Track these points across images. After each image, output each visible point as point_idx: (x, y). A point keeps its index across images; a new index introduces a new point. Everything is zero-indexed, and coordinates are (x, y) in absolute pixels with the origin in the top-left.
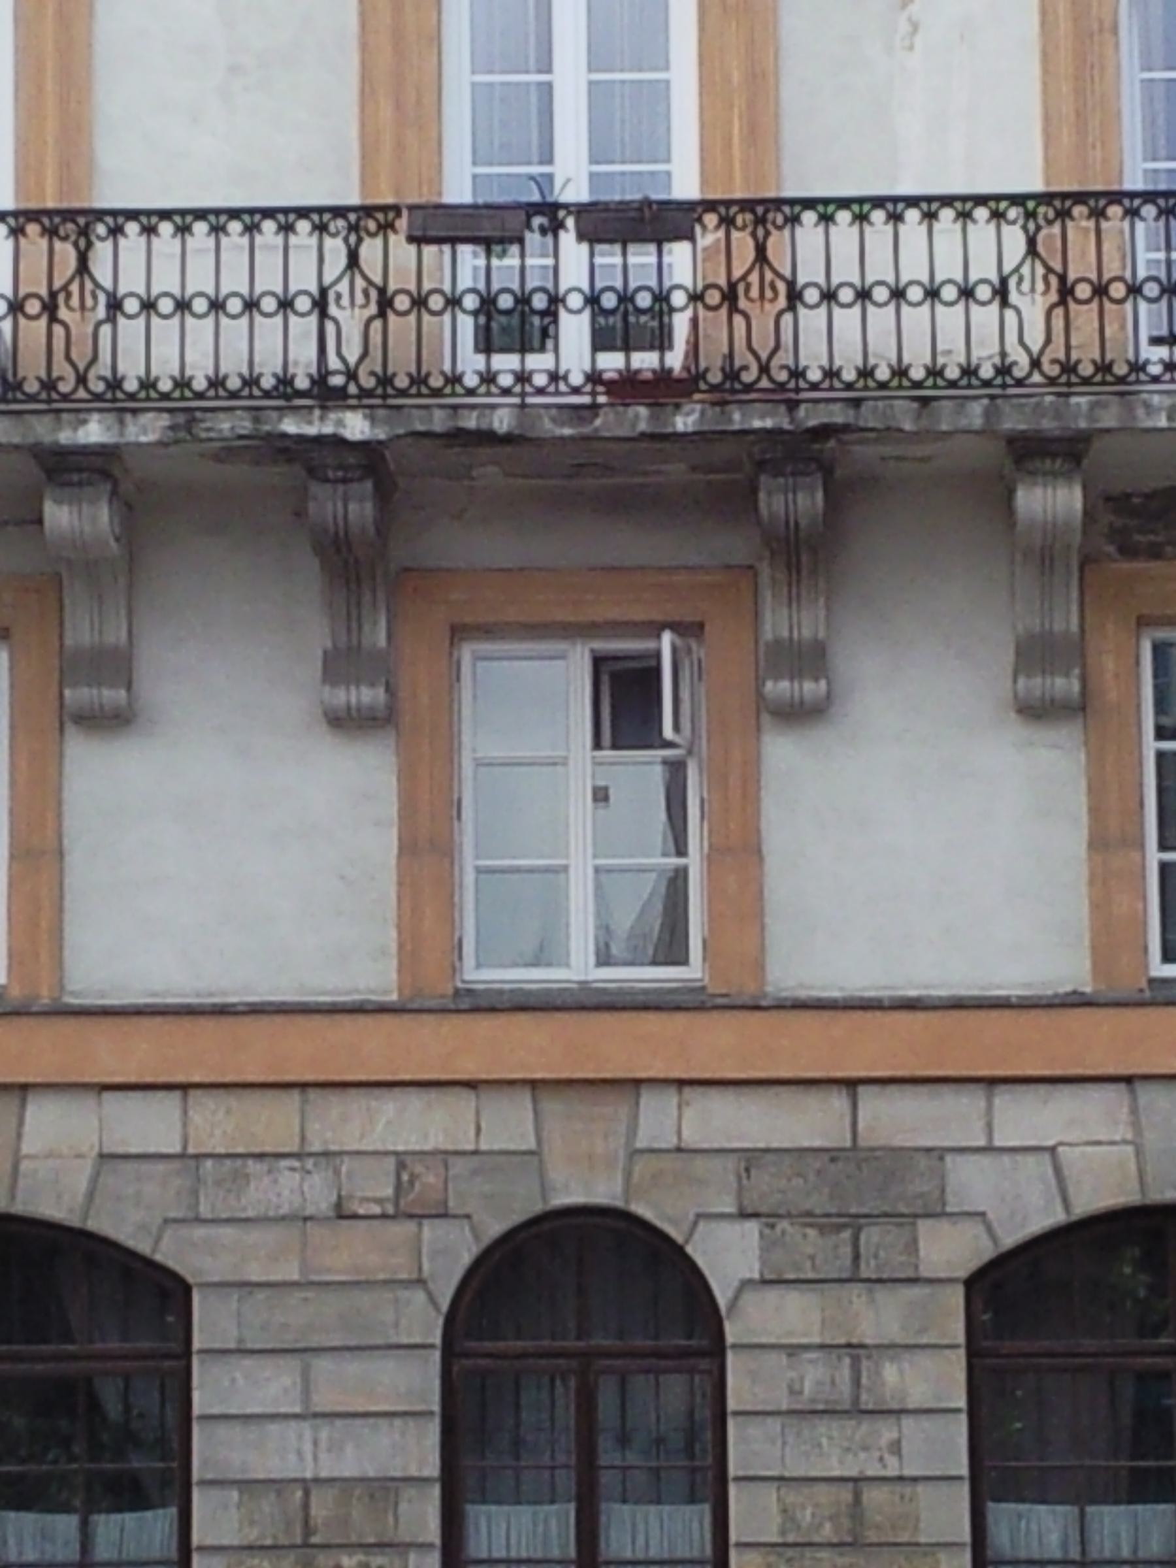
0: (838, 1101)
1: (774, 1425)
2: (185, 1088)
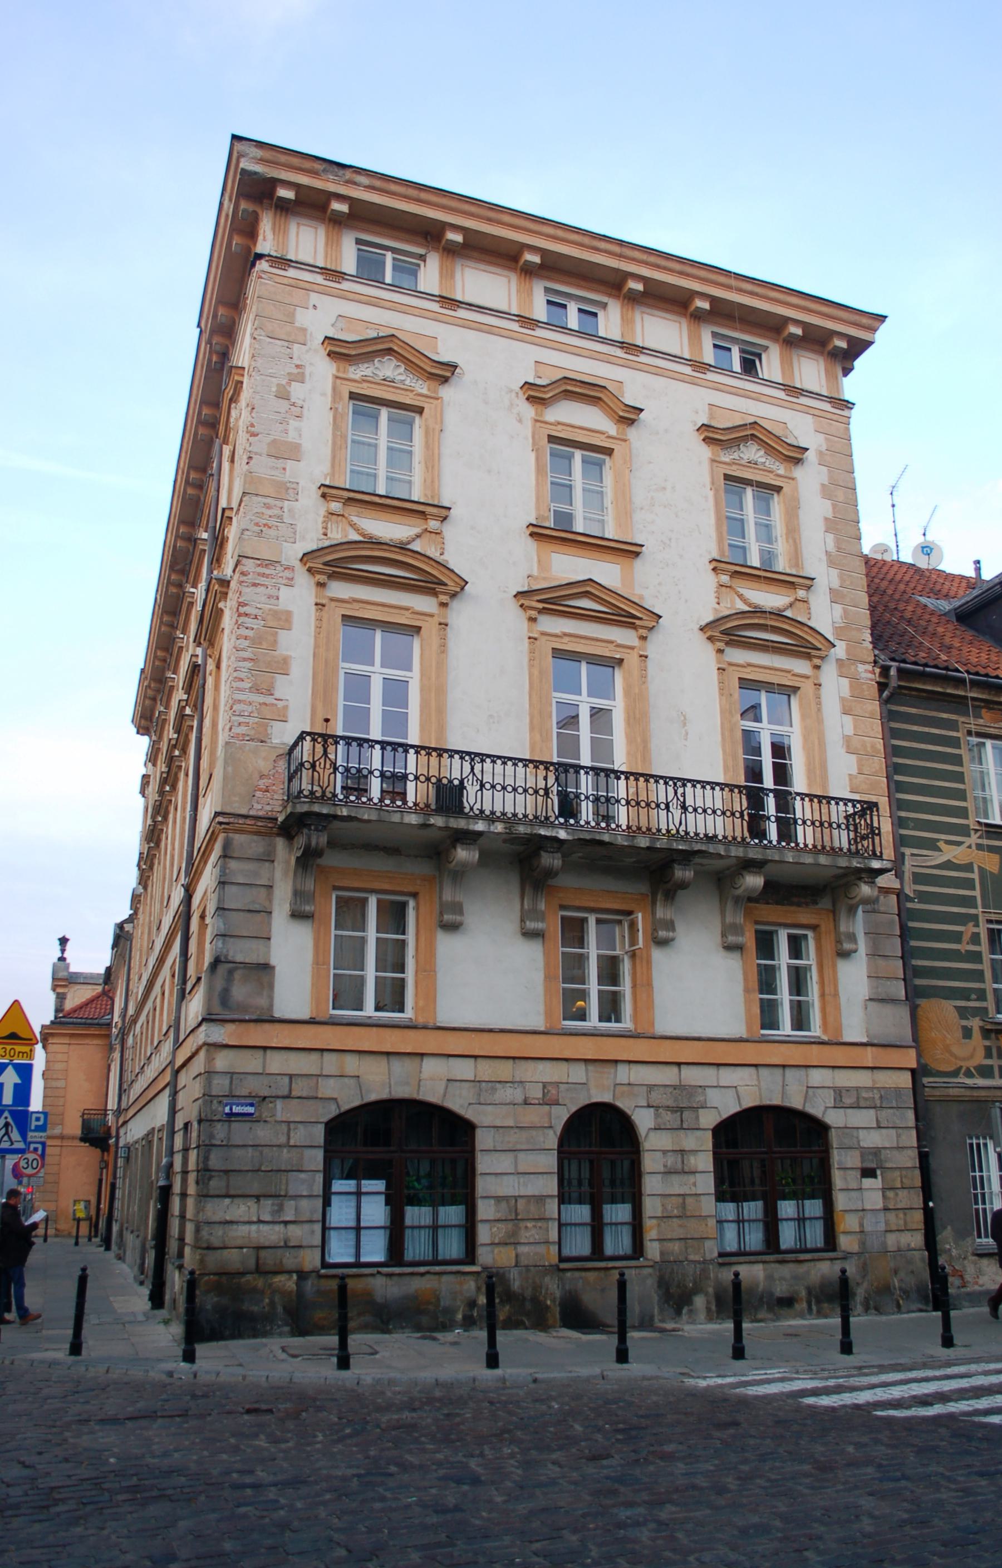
0: (675, 1069)
1: (659, 1177)
2: (475, 1057)
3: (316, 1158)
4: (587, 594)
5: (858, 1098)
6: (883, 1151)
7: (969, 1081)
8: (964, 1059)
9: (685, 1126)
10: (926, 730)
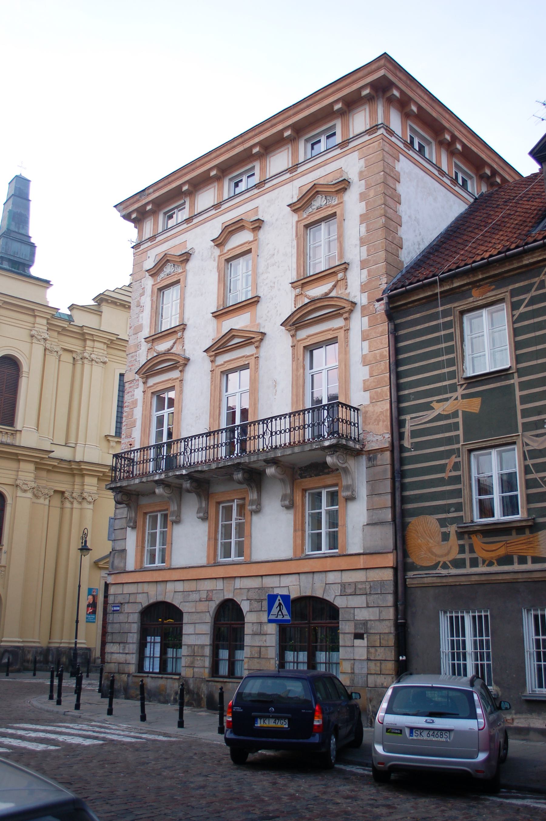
3: (135, 628)
4: (234, 337)
5: (355, 589)
6: (369, 622)
7: (444, 572)
8: (442, 556)
9: (263, 609)
10: (426, 325)
